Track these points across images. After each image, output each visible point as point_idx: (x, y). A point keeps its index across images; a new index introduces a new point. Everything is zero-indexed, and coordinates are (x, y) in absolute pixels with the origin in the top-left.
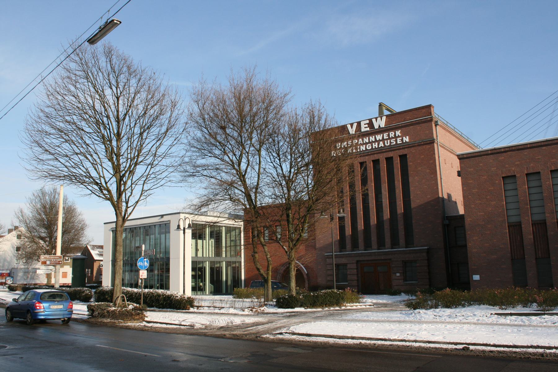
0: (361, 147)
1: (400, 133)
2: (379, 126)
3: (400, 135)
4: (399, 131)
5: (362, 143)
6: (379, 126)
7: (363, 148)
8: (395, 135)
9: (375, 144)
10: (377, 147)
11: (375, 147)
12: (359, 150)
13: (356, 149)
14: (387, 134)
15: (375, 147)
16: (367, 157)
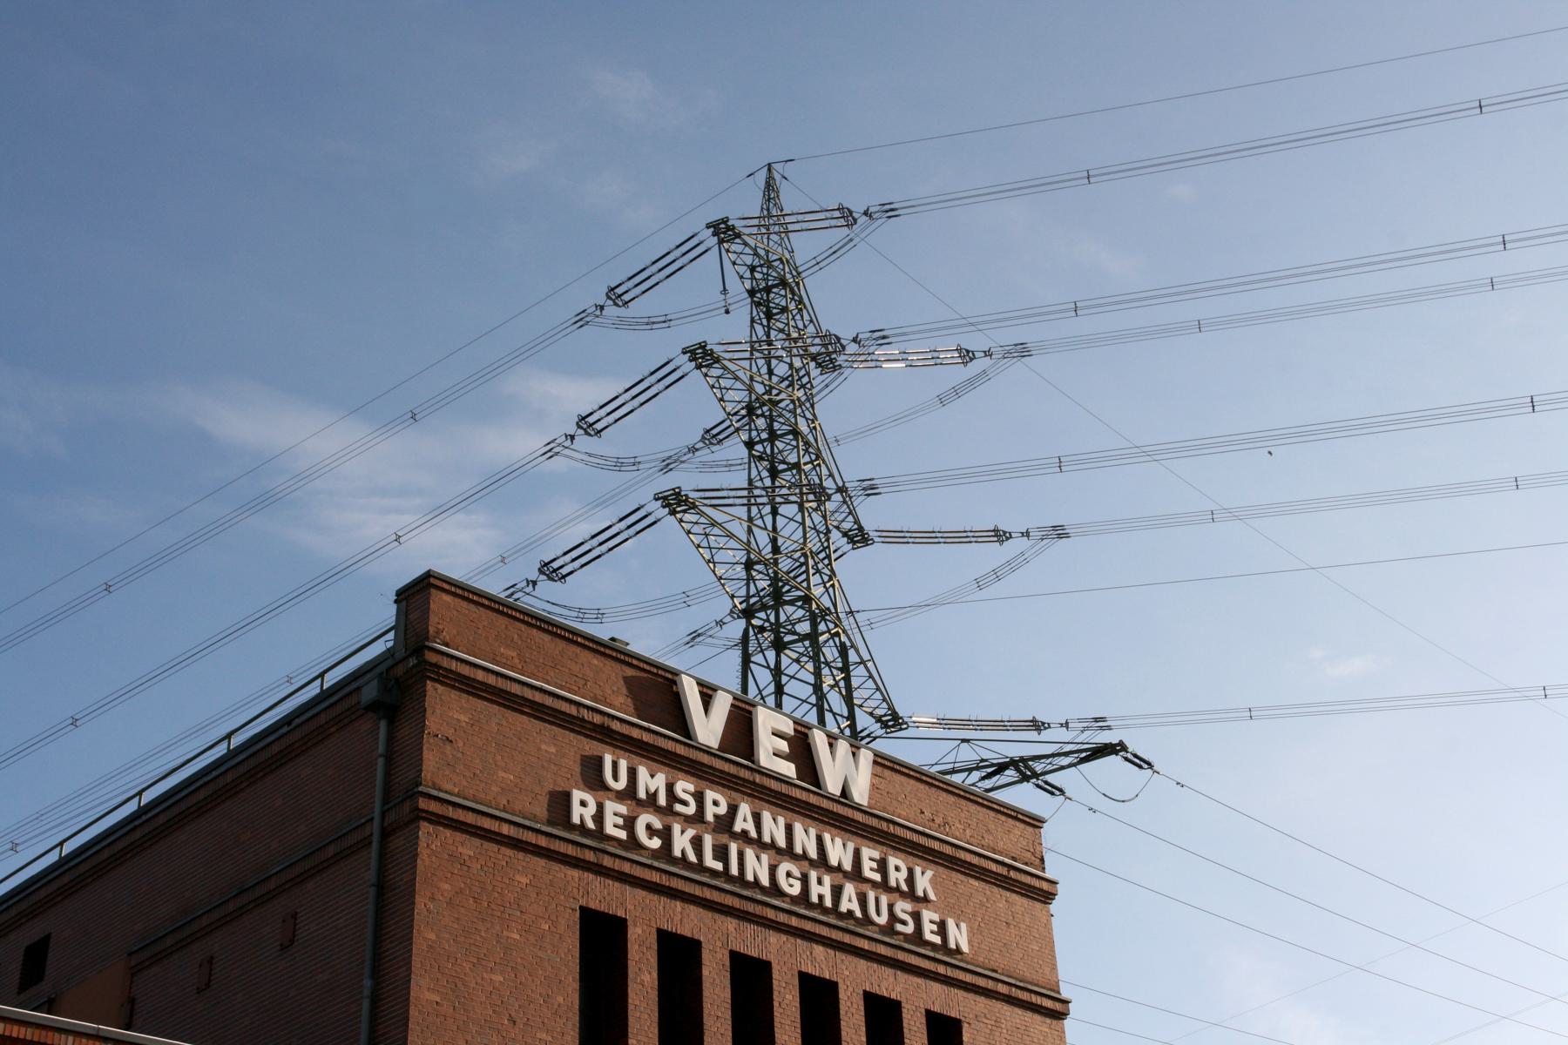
0: (750, 854)
1: (933, 881)
2: (845, 792)
3: (932, 896)
4: (929, 873)
5: (754, 834)
6: (845, 792)
7: (757, 867)
8: (910, 880)
9: (820, 882)
10: (828, 903)
11: (821, 897)
12: (734, 871)
13: (721, 853)
14: (876, 855)
15: (821, 897)
16: (774, 938)
